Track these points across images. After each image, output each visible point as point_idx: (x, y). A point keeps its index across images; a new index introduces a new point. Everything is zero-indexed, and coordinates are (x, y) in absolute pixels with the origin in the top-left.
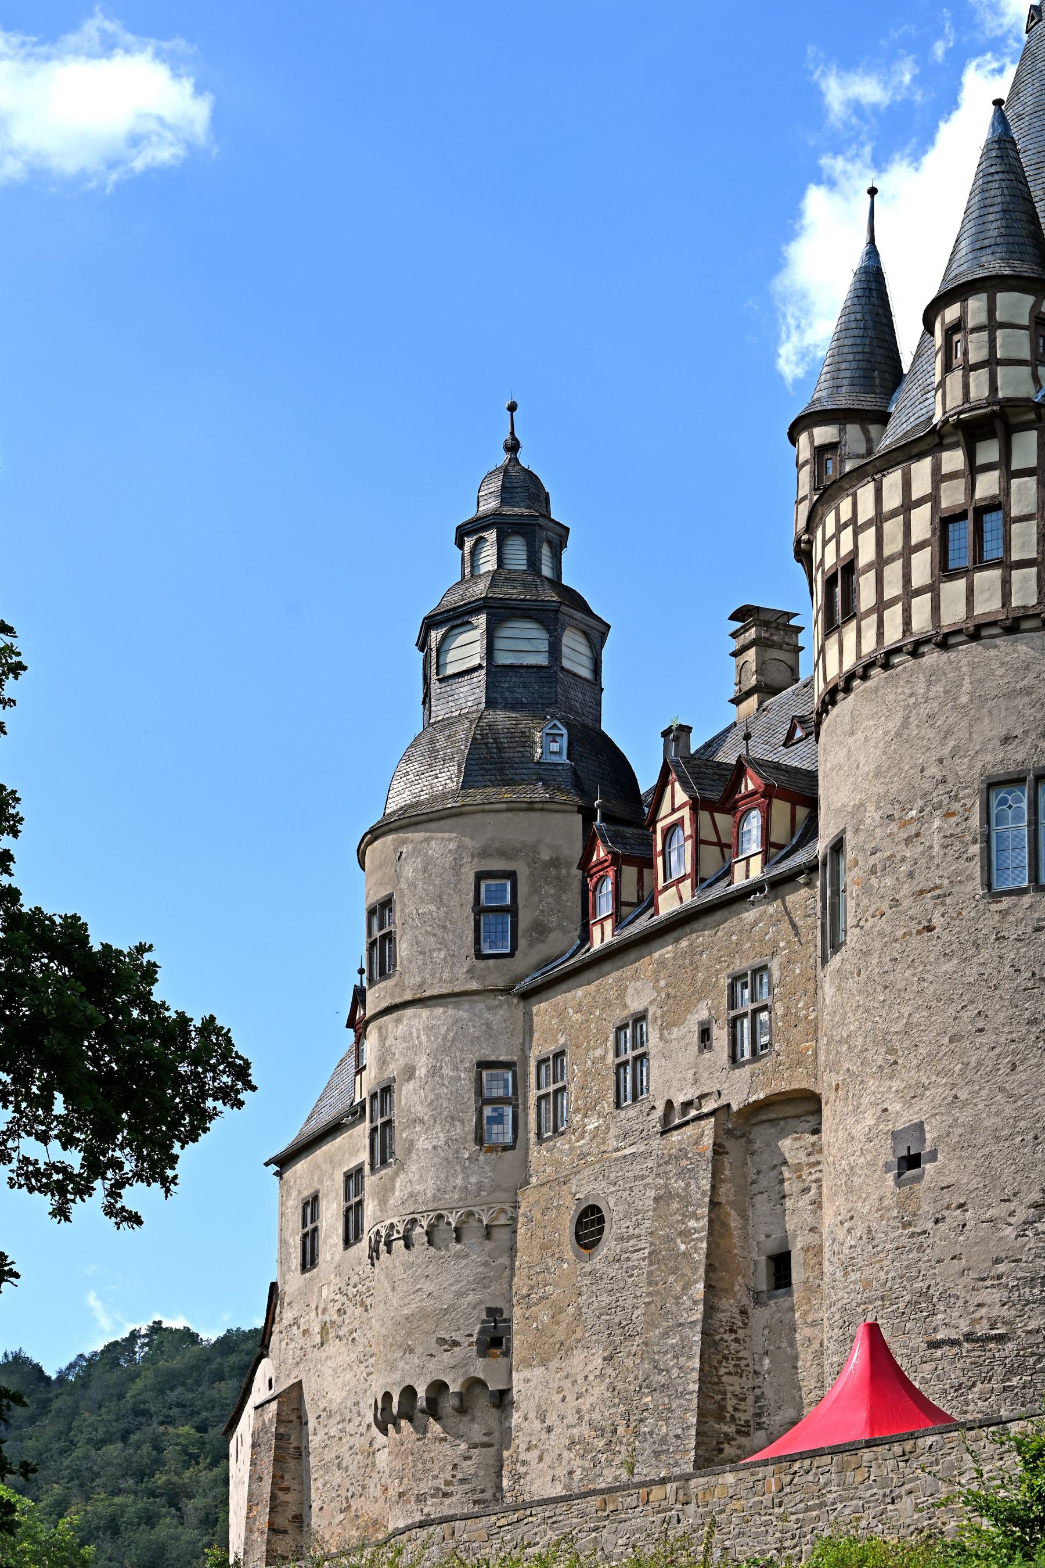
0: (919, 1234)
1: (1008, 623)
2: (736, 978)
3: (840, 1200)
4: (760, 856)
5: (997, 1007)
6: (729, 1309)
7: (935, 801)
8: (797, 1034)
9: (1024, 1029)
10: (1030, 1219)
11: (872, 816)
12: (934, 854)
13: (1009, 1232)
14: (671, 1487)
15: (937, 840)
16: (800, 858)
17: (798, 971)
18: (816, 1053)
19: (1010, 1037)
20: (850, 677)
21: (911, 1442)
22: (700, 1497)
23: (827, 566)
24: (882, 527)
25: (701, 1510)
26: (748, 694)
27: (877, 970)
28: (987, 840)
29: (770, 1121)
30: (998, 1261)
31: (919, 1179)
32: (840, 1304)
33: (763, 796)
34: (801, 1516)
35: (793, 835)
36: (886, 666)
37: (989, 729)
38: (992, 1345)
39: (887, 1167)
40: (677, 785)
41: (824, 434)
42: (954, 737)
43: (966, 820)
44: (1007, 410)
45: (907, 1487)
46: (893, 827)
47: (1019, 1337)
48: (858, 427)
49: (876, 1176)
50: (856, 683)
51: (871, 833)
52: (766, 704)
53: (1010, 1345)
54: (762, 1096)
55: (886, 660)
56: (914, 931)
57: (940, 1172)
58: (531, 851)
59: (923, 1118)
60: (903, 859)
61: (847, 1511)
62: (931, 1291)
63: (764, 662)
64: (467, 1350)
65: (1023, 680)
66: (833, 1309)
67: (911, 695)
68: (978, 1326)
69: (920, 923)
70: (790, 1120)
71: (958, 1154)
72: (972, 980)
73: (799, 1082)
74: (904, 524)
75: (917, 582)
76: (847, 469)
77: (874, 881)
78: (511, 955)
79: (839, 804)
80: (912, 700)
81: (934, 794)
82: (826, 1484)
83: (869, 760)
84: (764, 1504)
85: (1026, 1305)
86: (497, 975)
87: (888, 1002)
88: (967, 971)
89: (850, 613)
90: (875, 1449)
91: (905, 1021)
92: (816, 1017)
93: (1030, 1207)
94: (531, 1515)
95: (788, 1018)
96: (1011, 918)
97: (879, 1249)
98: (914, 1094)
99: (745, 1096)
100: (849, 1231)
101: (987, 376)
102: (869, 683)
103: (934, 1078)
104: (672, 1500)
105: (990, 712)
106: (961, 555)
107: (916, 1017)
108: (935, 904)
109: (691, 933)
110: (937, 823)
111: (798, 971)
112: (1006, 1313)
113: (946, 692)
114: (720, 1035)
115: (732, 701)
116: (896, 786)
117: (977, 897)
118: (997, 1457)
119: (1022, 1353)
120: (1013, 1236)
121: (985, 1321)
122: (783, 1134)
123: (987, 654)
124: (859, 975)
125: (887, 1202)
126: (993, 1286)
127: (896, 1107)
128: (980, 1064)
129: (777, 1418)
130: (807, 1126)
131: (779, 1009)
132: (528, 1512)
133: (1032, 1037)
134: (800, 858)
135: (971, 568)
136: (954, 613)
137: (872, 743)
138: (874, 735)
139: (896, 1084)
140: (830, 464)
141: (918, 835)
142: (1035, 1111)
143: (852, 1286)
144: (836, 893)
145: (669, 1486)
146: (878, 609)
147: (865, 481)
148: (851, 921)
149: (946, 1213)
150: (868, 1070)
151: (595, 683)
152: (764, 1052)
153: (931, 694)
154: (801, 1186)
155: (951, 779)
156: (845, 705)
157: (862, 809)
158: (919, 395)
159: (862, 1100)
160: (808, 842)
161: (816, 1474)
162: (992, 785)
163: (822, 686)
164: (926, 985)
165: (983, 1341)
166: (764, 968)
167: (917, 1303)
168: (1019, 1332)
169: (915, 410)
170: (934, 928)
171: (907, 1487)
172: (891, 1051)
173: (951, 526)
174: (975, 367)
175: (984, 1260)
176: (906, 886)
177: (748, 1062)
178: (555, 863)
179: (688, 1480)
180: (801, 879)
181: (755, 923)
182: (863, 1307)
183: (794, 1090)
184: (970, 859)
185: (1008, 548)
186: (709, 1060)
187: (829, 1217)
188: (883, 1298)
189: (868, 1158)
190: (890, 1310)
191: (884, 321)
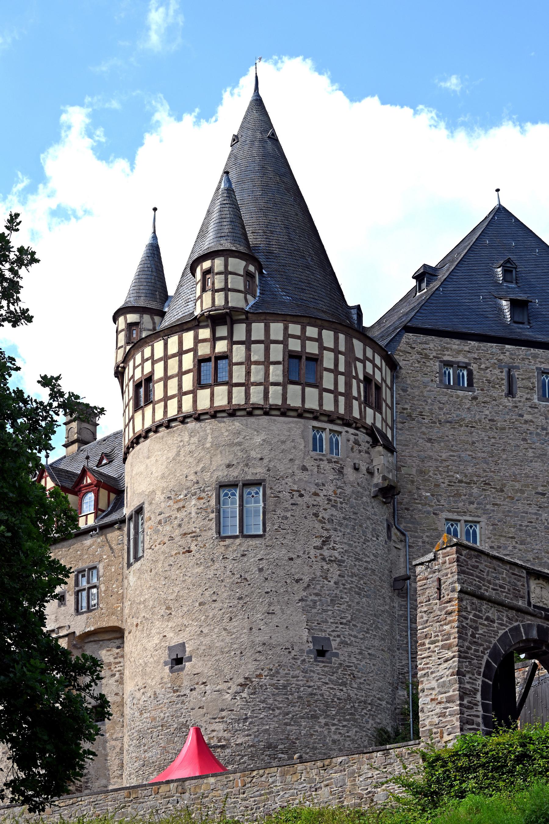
0: (182, 696)
1: (231, 411)
2: (79, 572)
3: (138, 679)
4: (93, 515)
5: (223, 590)
7: (193, 492)
8: (113, 600)
9: (236, 602)
10: (238, 691)
11: (159, 497)
12: (192, 516)
13: (228, 697)
14: (172, 786)
15: (194, 510)
16: (114, 517)
17: (113, 570)
18: (122, 609)
19: (229, 605)
20: (149, 431)
21: (329, 760)
22: (192, 790)
23: (136, 379)
24: (167, 362)
25: (193, 796)
26: (73, 443)
27: (161, 570)
28: (218, 511)
29: (95, 641)
30: (222, 710)
31: (182, 669)
32: (137, 729)
33: (95, 486)
34: (256, 798)
35: (108, 506)
36: (168, 427)
37: (219, 460)
38: (219, 750)
39: (166, 663)
40: (48, 479)
41: (132, 318)
42: (203, 462)
43: (208, 501)
44: (232, 313)
45: (325, 783)
46: (171, 502)
47: (232, 746)
48: (149, 316)
49: (159, 667)
50: (151, 434)
51: (158, 505)
52: (82, 448)
53: (228, 751)
54: (92, 629)
55: (168, 424)
56: (181, 552)
57: (193, 667)
59: (185, 641)
60: (176, 518)
61: (287, 796)
62: (188, 723)
63: (81, 429)
65: (237, 439)
66: (132, 731)
67: (181, 441)
68: (212, 741)
69: (184, 548)
70: (105, 642)
71: (202, 658)
72: (211, 577)
73: (113, 622)
74: (179, 361)
75: (185, 388)
76: (143, 336)
77: (160, 527)
79: (141, 491)
80: (181, 444)
81: (192, 488)
82: (273, 782)
83: (158, 470)
84: (234, 793)
85: (235, 732)
87: (167, 585)
88: (208, 572)
89: (149, 401)
90: (305, 764)
91: (176, 594)
92: (123, 592)
93: (238, 685)
94: (81, 801)
95: (107, 592)
96: (230, 549)
97: (160, 702)
99: (83, 628)
100: (143, 694)
101: (224, 295)
102: (158, 435)
103: (190, 622)
104: (173, 791)
105: (221, 452)
106: (207, 378)
107: (181, 593)
108: (192, 540)
109: (55, 549)
110: (193, 502)
111: (113, 570)
112: (226, 735)
113: (199, 441)
115: (63, 446)
116: (172, 484)
117: (214, 538)
118: (383, 767)
119: (233, 754)
120: (230, 699)
121: (215, 738)
122: (101, 648)
123: (219, 425)
124: (151, 571)
125: (165, 680)
126: (219, 722)
127: (170, 635)
128: (214, 616)
129: (96, 784)
130: (114, 644)
131: (103, 588)
132: (79, 799)
133: (240, 606)
134: (114, 517)
135: (213, 384)
137: (160, 462)
138: (161, 459)
139: (170, 624)
140: (135, 332)
141: (184, 507)
142: (241, 640)
143: (144, 720)
144: (136, 533)
145: (172, 785)
146: (165, 399)
147: (159, 339)
148: (147, 546)
149: (196, 686)
150: (155, 617)
152: (94, 608)
153: (192, 442)
154: (111, 673)
155: (201, 482)
156: (144, 445)
157: (154, 493)
158: (184, 303)
159: (152, 631)
160: (117, 510)
161: (267, 777)
162: (222, 486)
163: (131, 435)
164: (187, 578)
165: (214, 748)
166: (95, 568)
167: (180, 728)
168: (232, 744)
169: (182, 310)
170: (192, 551)
171: (325, 783)
172: (168, 608)
173: (202, 364)
174: (218, 291)
175: (215, 710)
176: (177, 531)
177: (85, 612)
179: (184, 781)
180: (116, 526)
181: (90, 546)
182: (151, 730)
183: (110, 627)
184: (210, 520)
185: (231, 376)
186: (64, 610)
187: (129, 687)
188: (162, 726)
189: (155, 659)
190: (166, 731)
191: (160, 269)
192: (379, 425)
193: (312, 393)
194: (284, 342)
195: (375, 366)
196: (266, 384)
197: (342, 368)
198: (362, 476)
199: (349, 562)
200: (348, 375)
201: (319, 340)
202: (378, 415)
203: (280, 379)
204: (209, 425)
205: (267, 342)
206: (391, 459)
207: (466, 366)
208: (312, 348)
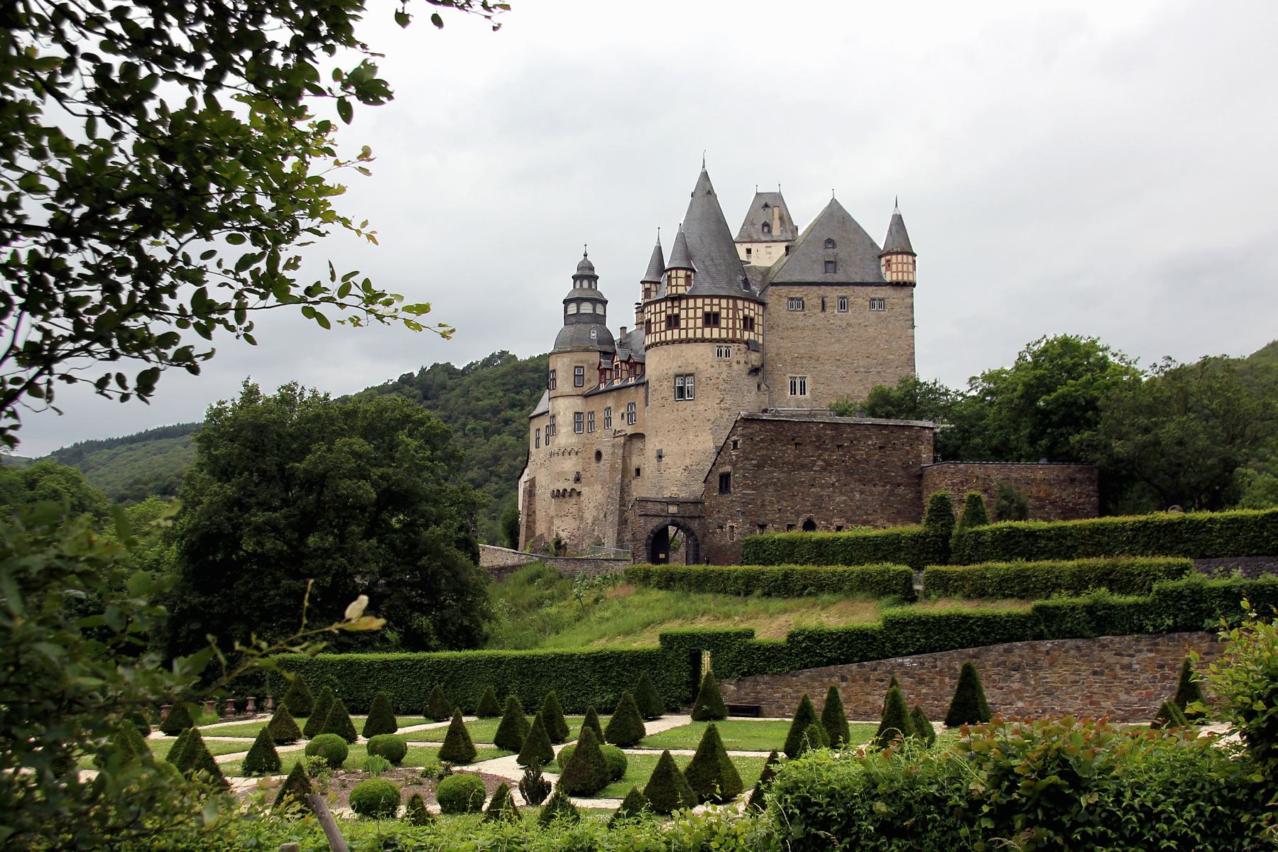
6: (626, 480)
11: (653, 378)
58: (587, 362)
64: (572, 482)
73: (640, 431)
86: (579, 391)
98: (661, 442)
114: (626, 416)
136: (669, 338)
151: (605, 316)
162: (677, 376)
192: (752, 338)
193: (716, 331)
194: (703, 308)
195: (750, 309)
196: (695, 328)
197: (731, 316)
198: (742, 365)
199: (733, 408)
200: (734, 319)
201: (719, 304)
202: (752, 334)
204: (670, 347)
205: (695, 308)
206: (758, 354)
207: (801, 299)
208: (716, 309)
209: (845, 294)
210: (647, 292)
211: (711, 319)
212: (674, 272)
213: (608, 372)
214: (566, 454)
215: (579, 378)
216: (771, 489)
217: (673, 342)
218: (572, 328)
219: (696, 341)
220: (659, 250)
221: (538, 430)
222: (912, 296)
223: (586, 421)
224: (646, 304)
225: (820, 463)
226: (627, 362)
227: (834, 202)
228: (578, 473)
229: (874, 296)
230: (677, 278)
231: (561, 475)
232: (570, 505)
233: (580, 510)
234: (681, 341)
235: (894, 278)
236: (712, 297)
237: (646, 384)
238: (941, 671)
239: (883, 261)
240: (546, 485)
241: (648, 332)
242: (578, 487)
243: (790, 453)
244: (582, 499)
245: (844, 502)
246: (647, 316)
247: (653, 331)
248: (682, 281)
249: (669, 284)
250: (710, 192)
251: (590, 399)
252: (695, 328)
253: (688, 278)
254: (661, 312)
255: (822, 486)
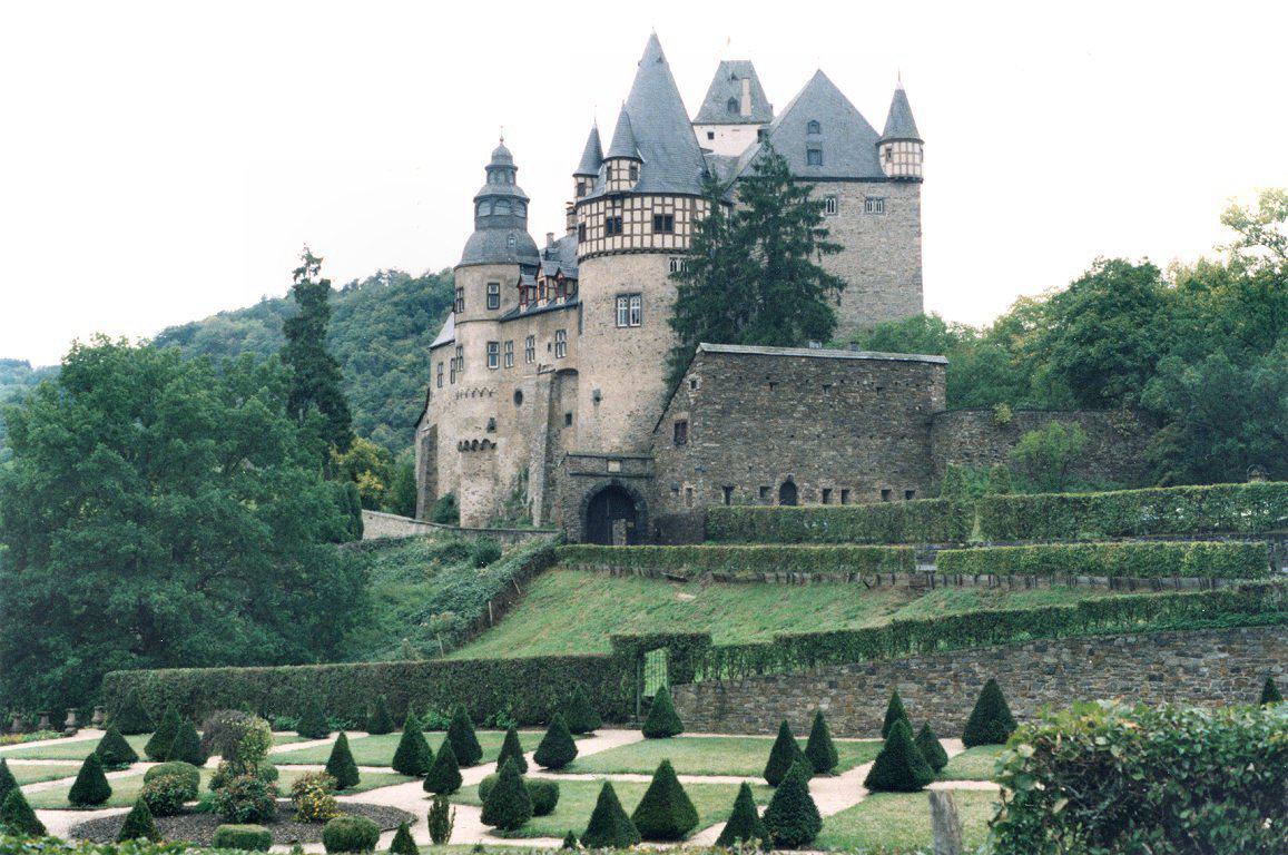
6: (555, 430)
58: (504, 277)
73: (572, 366)
78: (498, 308)
86: (494, 314)
112: (621, 445)
114: (553, 347)
162: (619, 296)
178: (511, 281)
194: (652, 209)
201: (673, 205)
203: (650, 232)
205: (643, 209)
208: (669, 211)
209: (833, 192)
210: (581, 188)
211: (663, 224)
212: (615, 163)
213: (531, 291)
214: (477, 395)
215: (493, 299)
216: (739, 441)
217: (615, 252)
218: (483, 234)
219: (643, 251)
220: (595, 136)
221: (441, 364)
222: (918, 195)
223: (502, 353)
224: (579, 204)
225: (801, 408)
226: (554, 278)
227: (819, 73)
228: (492, 419)
229: (870, 195)
230: (619, 170)
231: (470, 422)
232: (483, 460)
233: (494, 466)
234: (624, 252)
235: (897, 172)
236: (663, 195)
237: (578, 306)
238: (956, 675)
239: (882, 149)
240: (449, 437)
241: (582, 239)
242: (492, 438)
243: (764, 395)
244: (497, 453)
245: (833, 458)
246: (581, 220)
247: (588, 237)
248: (625, 175)
249: (609, 178)
250: (661, 60)
251: (507, 325)
252: (642, 235)
253: (633, 169)
254: (598, 214)
255: (806, 439)
